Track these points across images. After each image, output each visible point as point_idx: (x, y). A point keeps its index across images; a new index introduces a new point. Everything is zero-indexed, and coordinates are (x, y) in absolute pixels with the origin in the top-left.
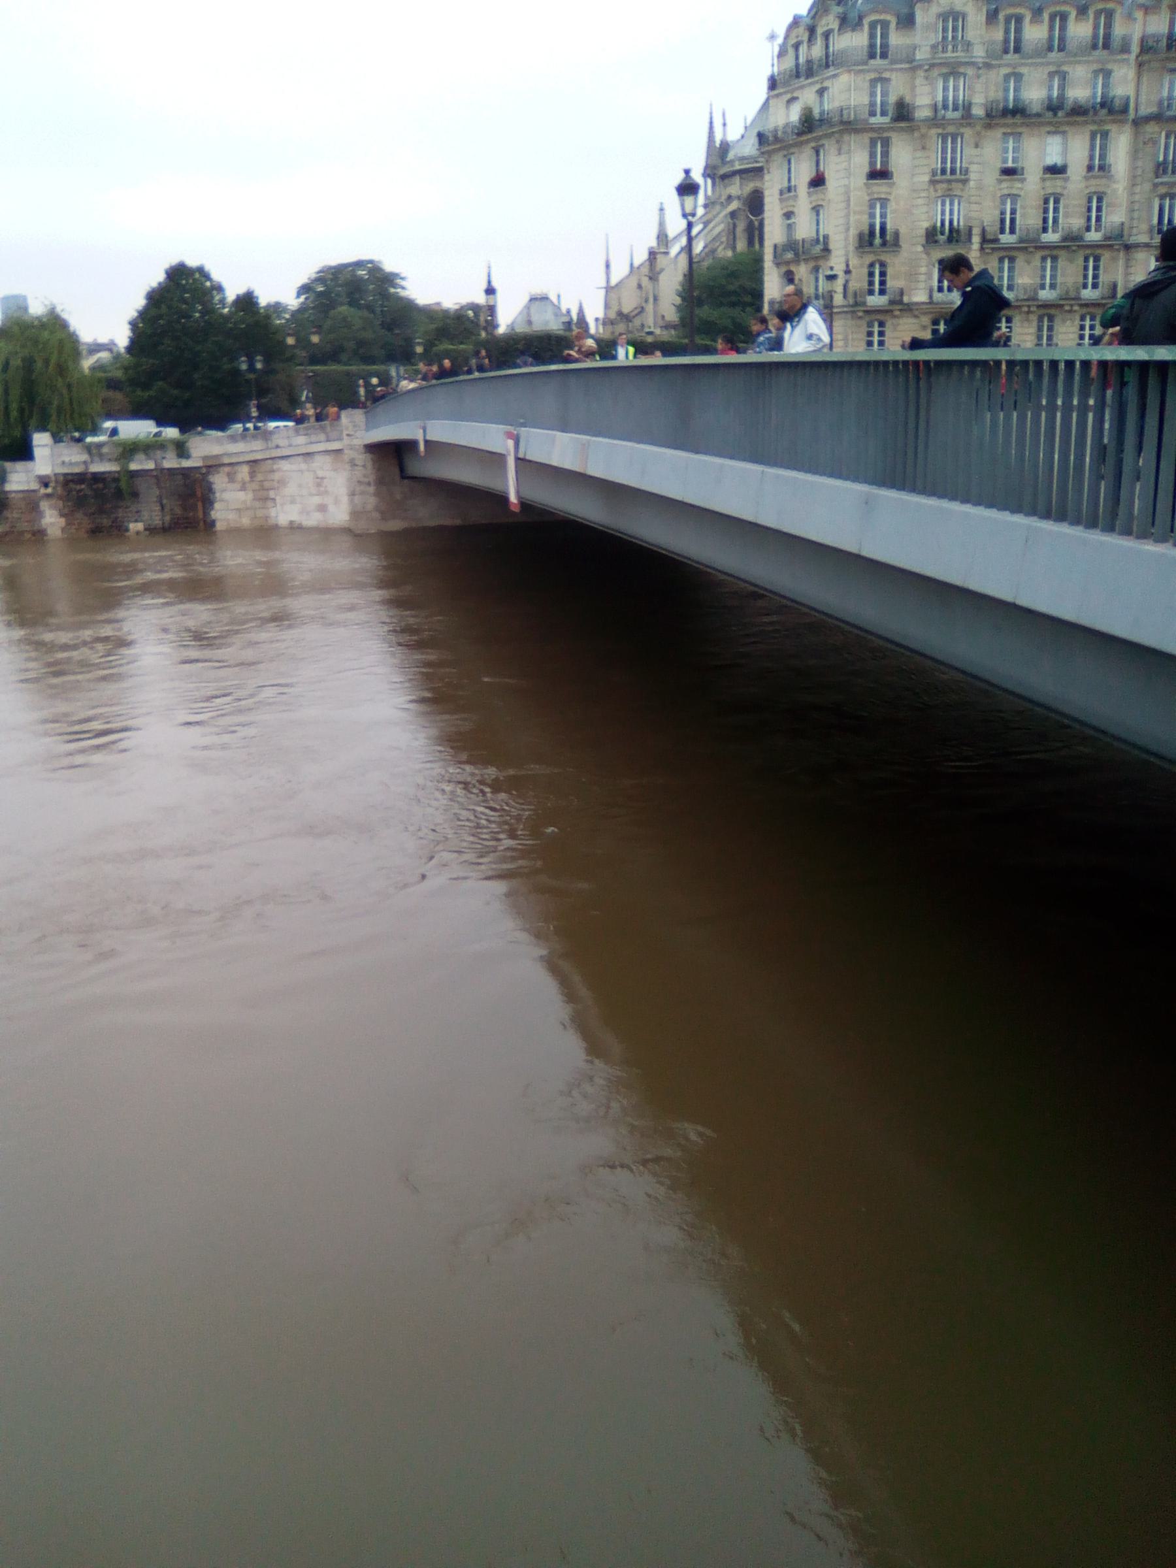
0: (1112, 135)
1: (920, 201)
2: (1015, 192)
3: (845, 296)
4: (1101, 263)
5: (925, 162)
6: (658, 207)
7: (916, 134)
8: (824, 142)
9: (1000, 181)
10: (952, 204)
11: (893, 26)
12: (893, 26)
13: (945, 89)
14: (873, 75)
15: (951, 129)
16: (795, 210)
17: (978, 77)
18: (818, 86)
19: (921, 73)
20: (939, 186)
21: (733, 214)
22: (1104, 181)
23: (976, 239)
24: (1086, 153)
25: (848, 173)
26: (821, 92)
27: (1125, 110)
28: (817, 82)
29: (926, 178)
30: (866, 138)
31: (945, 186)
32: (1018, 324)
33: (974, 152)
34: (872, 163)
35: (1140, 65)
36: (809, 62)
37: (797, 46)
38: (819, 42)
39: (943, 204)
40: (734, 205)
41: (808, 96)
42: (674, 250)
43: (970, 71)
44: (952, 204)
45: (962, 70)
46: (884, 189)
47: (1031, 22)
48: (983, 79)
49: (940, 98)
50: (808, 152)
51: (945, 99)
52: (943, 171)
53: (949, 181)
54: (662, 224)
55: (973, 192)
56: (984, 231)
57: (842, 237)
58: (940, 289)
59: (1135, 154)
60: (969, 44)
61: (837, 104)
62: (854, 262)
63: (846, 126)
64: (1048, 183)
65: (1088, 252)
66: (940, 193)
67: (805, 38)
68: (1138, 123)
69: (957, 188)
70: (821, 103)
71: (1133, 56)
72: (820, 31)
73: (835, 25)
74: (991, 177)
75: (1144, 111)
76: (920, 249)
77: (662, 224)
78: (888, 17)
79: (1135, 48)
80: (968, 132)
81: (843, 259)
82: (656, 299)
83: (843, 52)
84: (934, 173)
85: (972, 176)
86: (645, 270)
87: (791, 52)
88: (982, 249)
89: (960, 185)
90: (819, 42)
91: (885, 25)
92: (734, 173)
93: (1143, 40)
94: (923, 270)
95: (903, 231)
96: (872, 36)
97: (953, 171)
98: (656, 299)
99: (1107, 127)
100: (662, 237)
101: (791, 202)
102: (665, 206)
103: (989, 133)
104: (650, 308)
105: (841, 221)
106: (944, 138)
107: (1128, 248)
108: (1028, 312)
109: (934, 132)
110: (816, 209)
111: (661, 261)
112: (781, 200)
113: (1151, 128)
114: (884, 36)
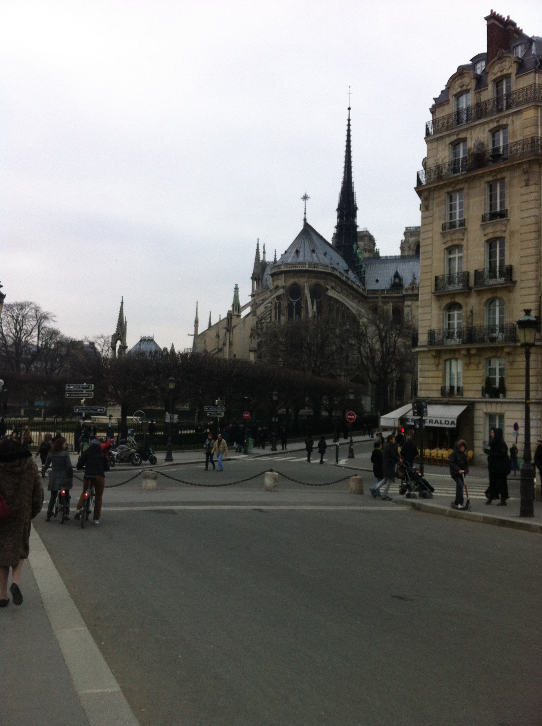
6: (234, 286)
16: (464, 243)
21: (278, 297)
28: (492, 121)
40: (280, 292)
42: (244, 314)
50: (481, 186)
54: (236, 297)
77: (236, 297)
82: (231, 344)
86: (225, 324)
92: (281, 273)
98: (231, 344)
100: (236, 306)
102: (239, 287)
104: (227, 348)
111: (235, 321)
112: (444, 235)
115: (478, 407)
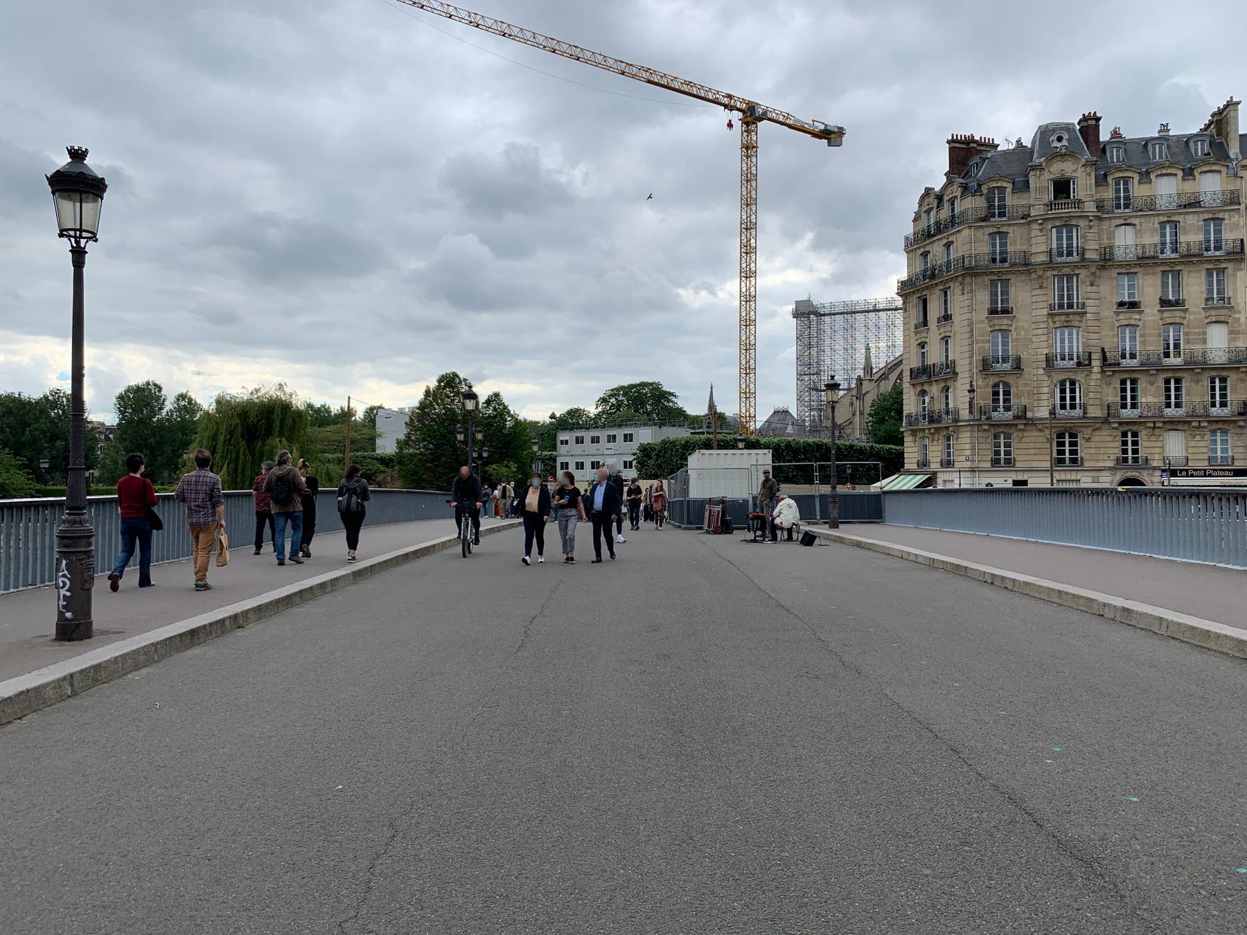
1: (1040, 332)
2: (1132, 322)
3: (971, 412)
4: (1184, 385)
5: (1045, 298)
7: (1033, 276)
8: (951, 284)
9: (1118, 314)
10: (1071, 334)
11: (1009, 190)
12: (1009, 190)
13: (1059, 238)
14: (992, 230)
15: (1066, 271)
17: (1090, 227)
18: (945, 241)
19: (1035, 226)
20: (1056, 319)
23: (1096, 363)
24: (1204, 288)
25: (971, 309)
26: (948, 245)
29: (1045, 312)
30: (987, 279)
31: (1063, 318)
32: (1145, 438)
33: (1089, 289)
34: (994, 301)
36: (938, 223)
37: (928, 212)
38: (946, 205)
39: (1062, 334)
41: (937, 250)
43: (1082, 223)
44: (1071, 334)
45: (1074, 223)
46: (1005, 321)
47: (1140, 182)
48: (1095, 230)
49: (1054, 246)
51: (1060, 247)
52: (1061, 306)
53: (1067, 314)
55: (1090, 323)
56: (1104, 358)
57: (967, 361)
58: (1063, 407)
60: (1080, 201)
61: (960, 254)
62: (979, 382)
63: (969, 271)
64: (1166, 315)
65: (1214, 373)
66: (1058, 325)
67: (935, 205)
69: (1075, 320)
70: (948, 254)
72: (946, 198)
73: (959, 193)
74: (1109, 311)
76: (1041, 371)
78: (1005, 185)
80: (1083, 273)
81: (968, 381)
83: (963, 213)
84: (1052, 307)
85: (1088, 309)
87: (924, 216)
88: (1103, 372)
89: (1078, 318)
90: (946, 205)
91: (1002, 190)
94: (1046, 390)
95: (1024, 356)
97: (1070, 306)
99: (1223, 265)
101: (924, 334)
103: (1104, 273)
105: (966, 348)
106: (1061, 277)
108: (1154, 428)
109: (1049, 273)
110: (945, 340)
112: (916, 333)
114: (1002, 199)
115: (939, 475)
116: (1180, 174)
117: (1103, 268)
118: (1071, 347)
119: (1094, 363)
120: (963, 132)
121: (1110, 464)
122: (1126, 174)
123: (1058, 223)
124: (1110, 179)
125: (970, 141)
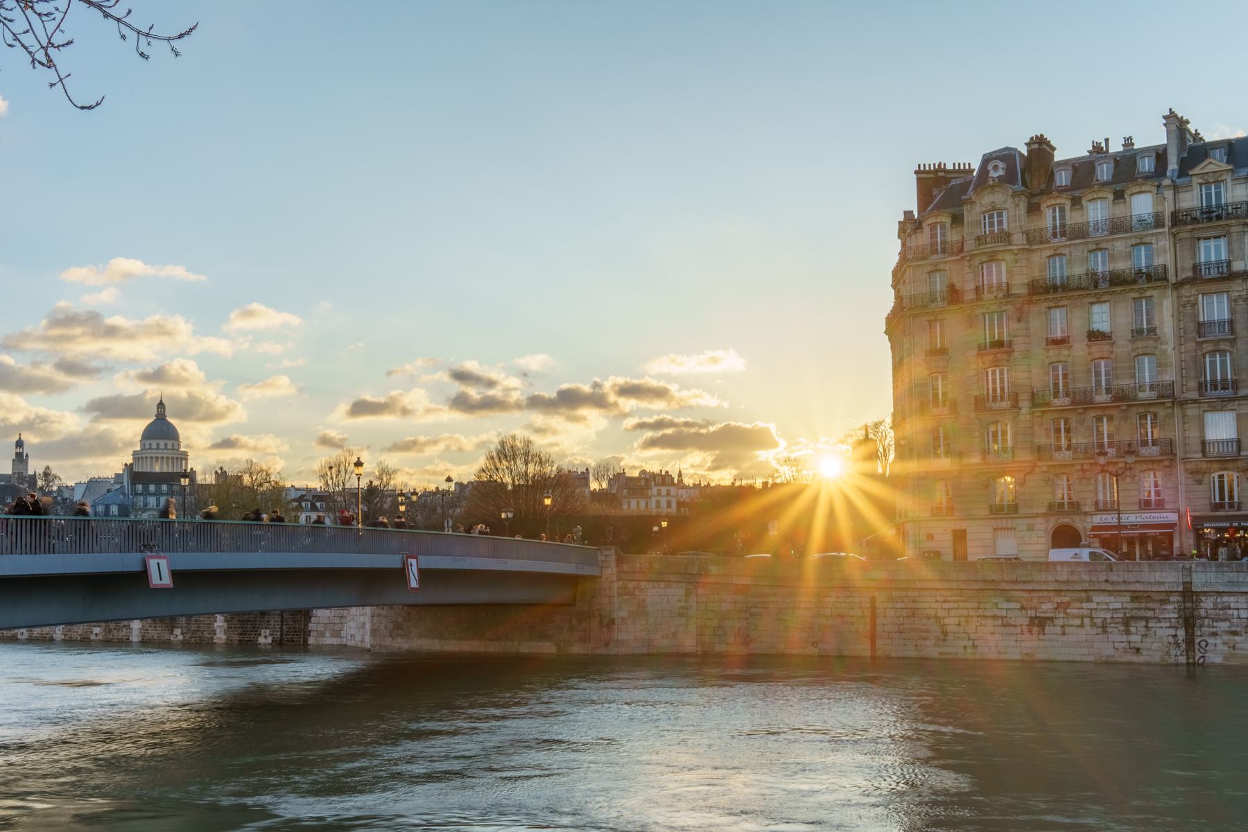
0: (1155, 300)
2: (1062, 358)
9: (1047, 351)
14: (929, 268)
17: (1016, 261)
22: (1151, 342)
27: (1166, 279)
35: (1174, 236)
47: (1072, 209)
59: (1178, 316)
64: (1094, 349)
68: (1178, 286)
71: (1166, 230)
75: (1182, 276)
78: (944, 219)
79: (1168, 223)
85: (1016, 347)
93: (1174, 215)
96: (933, 236)
99: (1148, 293)
107: (1183, 403)
113: (1187, 291)
116: (1111, 197)
117: (1030, 302)
118: (1002, 389)
119: (1021, 404)
120: (930, 160)
121: (1043, 510)
122: (1058, 201)
123: (985, 259)
124: (925, 225)
125: (940, 169)
